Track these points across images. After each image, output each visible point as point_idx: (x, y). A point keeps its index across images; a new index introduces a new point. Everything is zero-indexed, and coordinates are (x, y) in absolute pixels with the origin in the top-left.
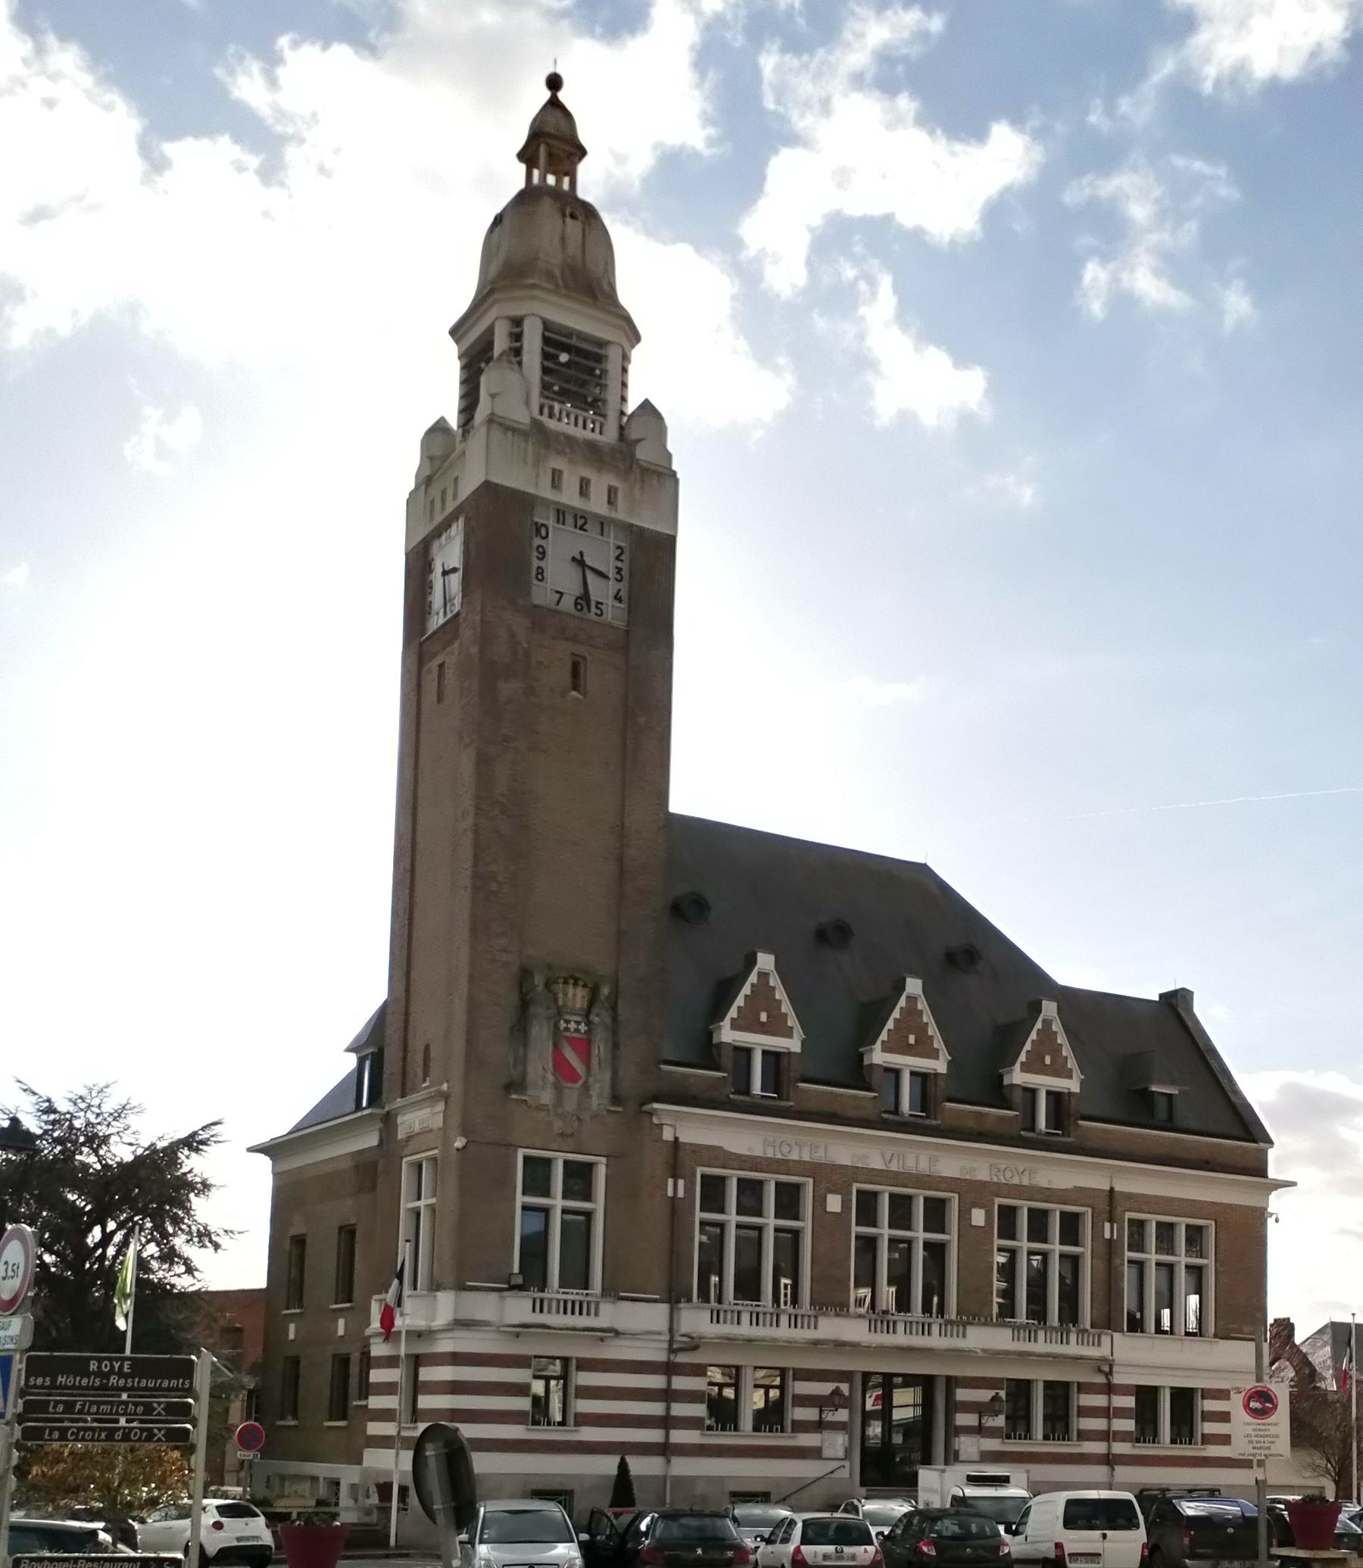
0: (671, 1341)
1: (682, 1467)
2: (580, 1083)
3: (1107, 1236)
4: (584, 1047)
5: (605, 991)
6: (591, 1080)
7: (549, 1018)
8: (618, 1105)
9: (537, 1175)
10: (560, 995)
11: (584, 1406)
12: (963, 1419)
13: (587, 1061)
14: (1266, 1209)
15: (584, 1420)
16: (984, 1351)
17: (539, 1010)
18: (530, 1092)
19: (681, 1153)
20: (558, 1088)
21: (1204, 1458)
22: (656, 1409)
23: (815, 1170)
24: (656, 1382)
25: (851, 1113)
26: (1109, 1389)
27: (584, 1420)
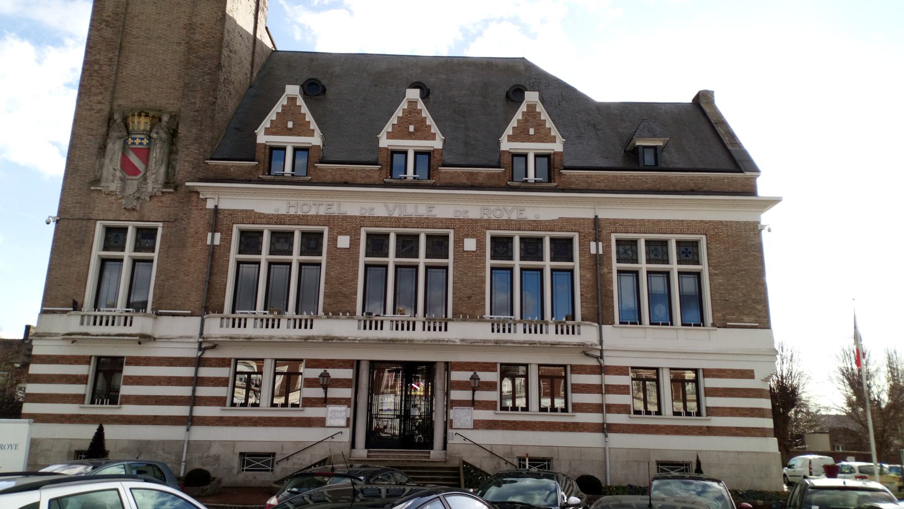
0: (200, 343)
1: (200, 433)
2: (141, 175)
3: (593, 251)
4: (144, 154)
5: (165, 118)
6: (148, 174)
8: (169, 187)
12: (456, 395)
13: (146, 162)
14: (758, 223)
16: (462, 340)
17: (114, 134)
18: (102, 184)
19: (221, 216)
20: (123, 180)
21: (708, 427)
22: (185, 391)
23: (328, 220)
24: (187, 372)
25: (359, 181)
26: (602, 370)
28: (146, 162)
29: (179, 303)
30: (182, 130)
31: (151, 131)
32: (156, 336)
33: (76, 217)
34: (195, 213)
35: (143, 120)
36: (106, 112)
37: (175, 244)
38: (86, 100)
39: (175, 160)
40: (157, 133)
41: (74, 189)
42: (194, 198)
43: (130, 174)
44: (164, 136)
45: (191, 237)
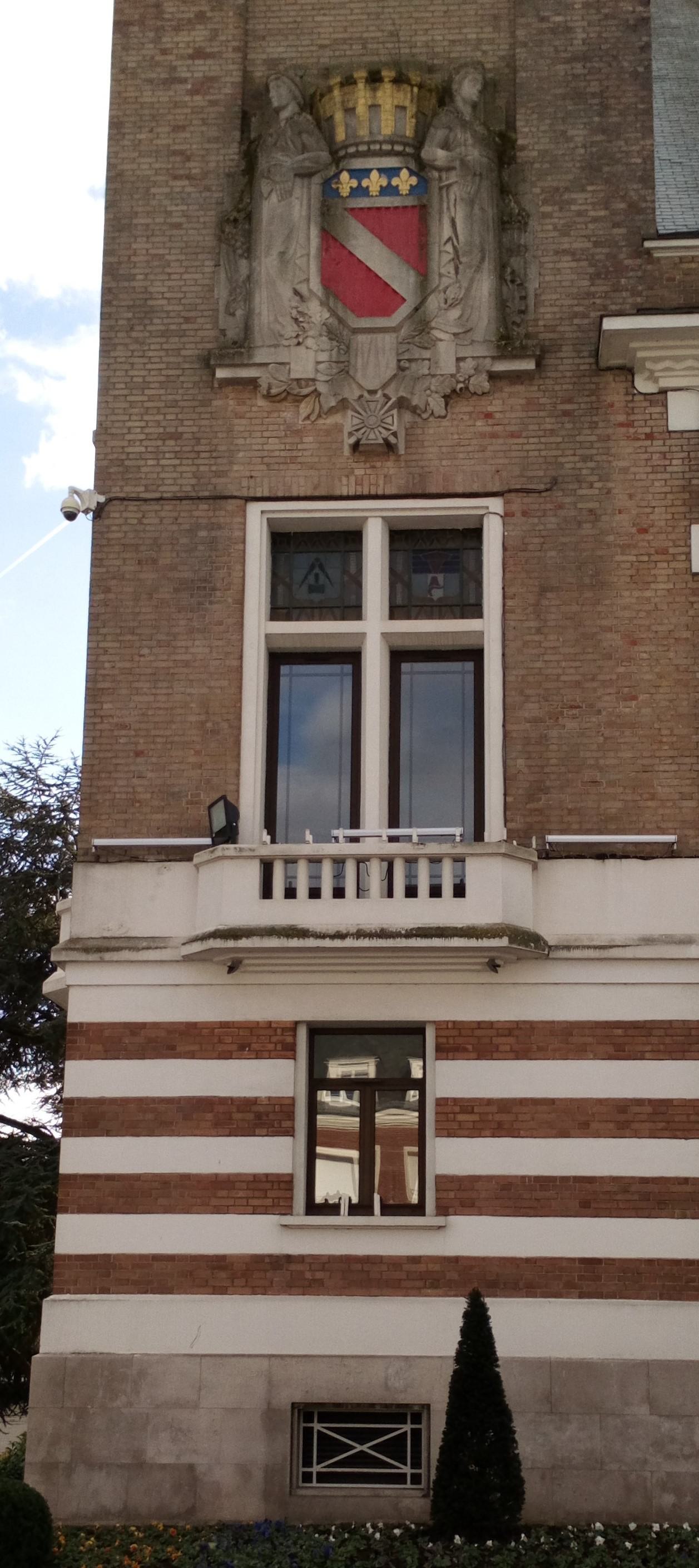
2: (403, 311)
4: (410, 230)
5: (468, 89)
6: (434, 302)
7: (305, 175)
8: (520, 354)
9: (313, 564)
10: (339, 116)
11: (455, 1156)
13: (418, 257)
15: (465, 1196)
17: (281, 160)
18: (260, 356)
20: (337, 335)
27: (465, 1196)
28: (418, 257)
29: (613, 807)
30: (532, 136)
31: (420, 141)
32: (550, 934)
33: (169, 490)
34: (625, 453)
35: (388, 96)
36: (228, 88)
37: (559, 580)
38: (149, 49)
39: (519, 250)
40: (446, 146)
41: (145, 385)
42: (614, 392)
43: (360, 312)
44: (474, 154)
45: (625, 548)
